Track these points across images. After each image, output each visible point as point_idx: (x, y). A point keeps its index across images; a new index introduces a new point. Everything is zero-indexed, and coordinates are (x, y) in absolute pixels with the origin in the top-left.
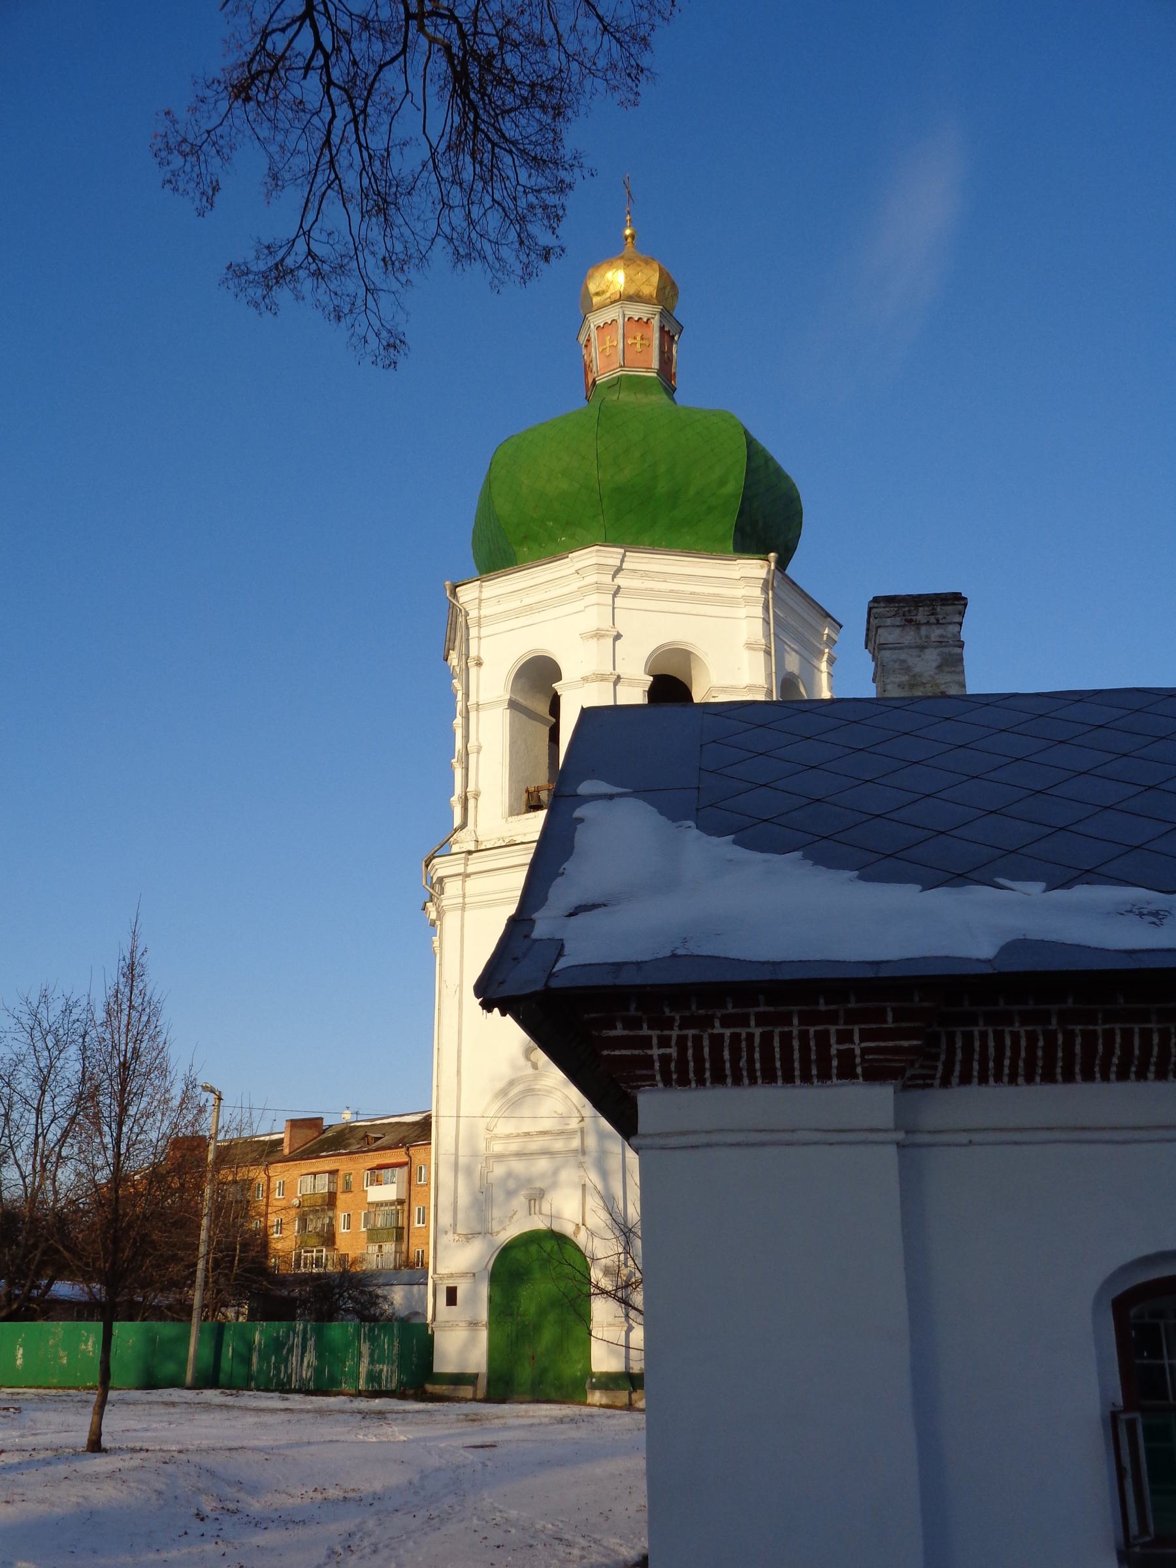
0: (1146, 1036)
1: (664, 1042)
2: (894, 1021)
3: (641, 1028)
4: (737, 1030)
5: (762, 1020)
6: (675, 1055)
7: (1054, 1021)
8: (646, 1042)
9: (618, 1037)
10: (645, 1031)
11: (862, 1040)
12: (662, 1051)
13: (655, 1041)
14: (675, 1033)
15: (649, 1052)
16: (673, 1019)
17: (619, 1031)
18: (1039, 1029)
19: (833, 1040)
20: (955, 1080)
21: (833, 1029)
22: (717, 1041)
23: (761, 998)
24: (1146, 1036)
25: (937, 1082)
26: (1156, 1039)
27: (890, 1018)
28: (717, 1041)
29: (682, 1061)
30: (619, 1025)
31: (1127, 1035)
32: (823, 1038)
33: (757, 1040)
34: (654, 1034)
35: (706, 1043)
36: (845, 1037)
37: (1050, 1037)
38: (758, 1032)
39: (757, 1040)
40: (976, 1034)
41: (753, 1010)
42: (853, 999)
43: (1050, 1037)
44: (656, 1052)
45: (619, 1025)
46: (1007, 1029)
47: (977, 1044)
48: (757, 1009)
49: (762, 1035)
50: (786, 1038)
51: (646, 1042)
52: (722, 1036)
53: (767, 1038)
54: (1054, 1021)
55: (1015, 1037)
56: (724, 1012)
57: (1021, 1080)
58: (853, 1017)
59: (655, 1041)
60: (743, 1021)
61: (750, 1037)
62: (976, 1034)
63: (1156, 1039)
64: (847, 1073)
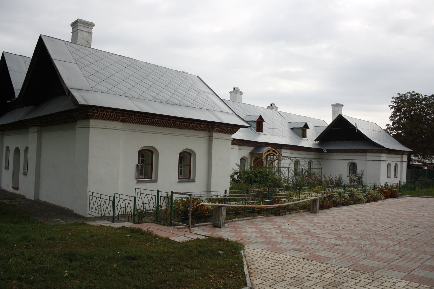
0: (150, 120)
1: (97, 113)
2: (126, 115)
3: (91, 110)
4: (107, 113)
5: (111, 112)
6: (98, 115)
7: (141, 117)
8: (95, 113)
9: (91, 112)
10: (95, 111)
11: (122, 116)
12: (97, 114)
13: (96, 113)
14: (99, 112)
15: (95, 114)
16: (99, 110)
17: (92, 111)
18: (139, 117)
19: (118, 116)
20: (127, 122)
21: (118, 115)
22: (104, 114)
23: (166, 117)
24: (150, 120)
25: (125, 122)
26: (151, 120)
27: (126, 114)
28: (104, 114)
29: (98, 116)
30: (92, 110)
31: (148, 119)
32: (117, 115)
33: (109, 115)
34: (96, 112)
35: (103, 114)
36: (120, 116)
37: (140, 119)
38: (134, 117)
39: (109, 115)
40: (114, 115)
41: (109, 111)
42: (158, 116)
43: (140, 119)
44: (96, 114)
45: (92, 110)
46: (136, 117)
47: (132, 118)
48: (110, 111)
49: (110, 114)
50: (113, 115)
51: (95, 113)
52: (105, 113)
53: (110, 114)
54: (141, 117)
55: (136, 118)
56: (142, 115)
57: (135, 123)
58: (121, 113)
59: (96, 113)
60: (108, 112)
61: (108, 114)
62: (114, 115)
63: (151, 120)
64: (118, 121)
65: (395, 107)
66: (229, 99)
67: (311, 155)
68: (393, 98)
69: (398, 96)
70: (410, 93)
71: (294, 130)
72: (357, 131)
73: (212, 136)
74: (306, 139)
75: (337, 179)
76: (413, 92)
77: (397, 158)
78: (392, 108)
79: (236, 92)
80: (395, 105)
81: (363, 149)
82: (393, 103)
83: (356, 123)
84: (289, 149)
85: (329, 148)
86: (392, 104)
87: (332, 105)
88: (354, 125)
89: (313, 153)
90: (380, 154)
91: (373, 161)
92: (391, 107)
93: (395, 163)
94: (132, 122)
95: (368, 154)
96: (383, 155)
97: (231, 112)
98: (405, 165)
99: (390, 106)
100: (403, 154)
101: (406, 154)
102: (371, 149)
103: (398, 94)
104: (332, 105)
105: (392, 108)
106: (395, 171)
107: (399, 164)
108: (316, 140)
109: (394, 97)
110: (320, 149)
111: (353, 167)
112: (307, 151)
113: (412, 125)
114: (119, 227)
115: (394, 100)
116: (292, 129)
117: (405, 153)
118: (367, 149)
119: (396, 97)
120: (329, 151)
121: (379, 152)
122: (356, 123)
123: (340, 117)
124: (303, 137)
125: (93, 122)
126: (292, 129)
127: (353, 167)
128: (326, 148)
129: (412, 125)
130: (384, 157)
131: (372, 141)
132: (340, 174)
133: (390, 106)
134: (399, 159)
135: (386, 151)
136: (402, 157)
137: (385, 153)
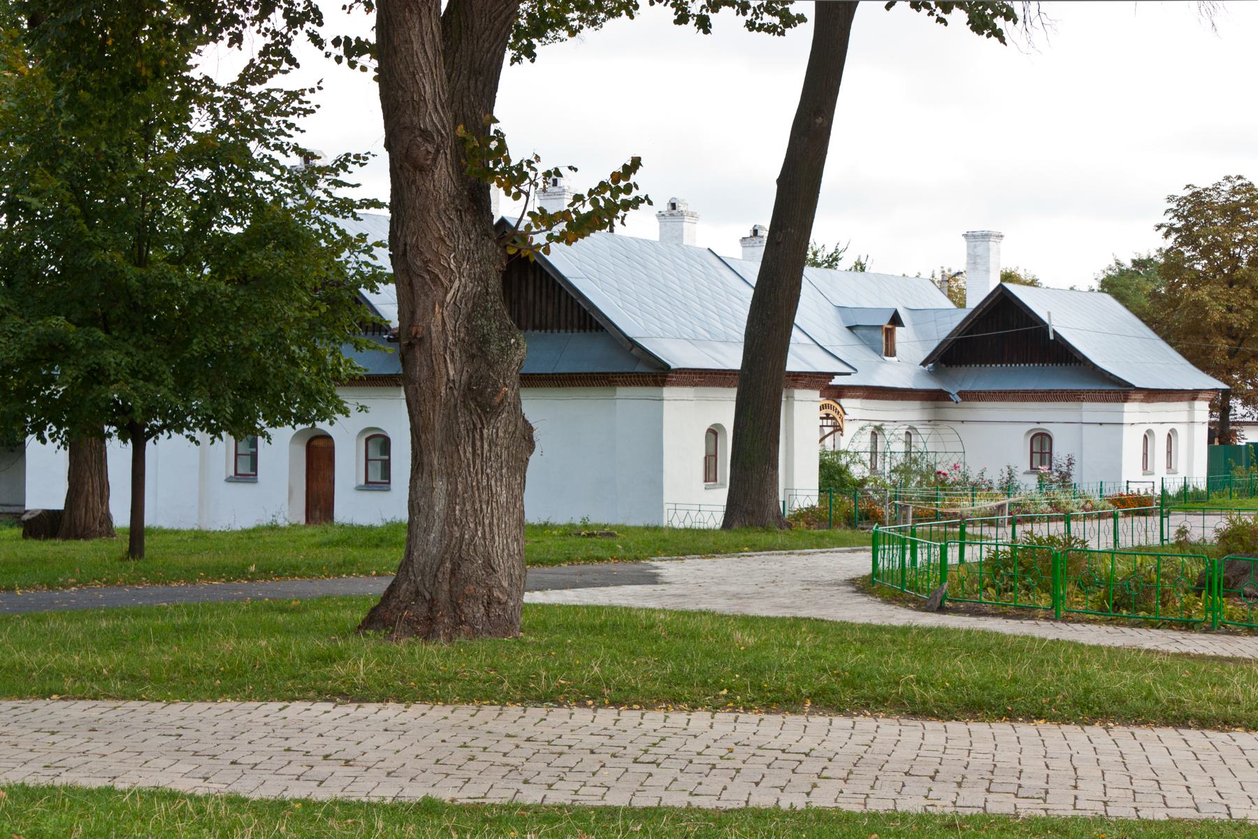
65: (1177, 230)
66: (657, 238)
67: (911, 412)
68: (1170, 199)
69: (1188, 193)
70: (1227, 178)
71: (858, 332)
72: (1052, 337)
73: (793, 397)
74: (895, 359)
75: (1005, 480)
76: (1240, 177)
77: (1175, 412)
78: (1167, 235)
79: (682, 214)
80: (1179, 224)
81: (1072, 391)
82: (1172, 215)
83: (1049, 313)
84: (857, 397)
85: (968, 386)
86: (1166, 220)
87: (966, 236)
88: (1045, 318)
89: (916, 404)
90: (1121, 404)
91: (1101, 424)
92: (1164, 230)
93: (1167, 428)
94: (841, 412)
95: (1086, 405)
96: (1128, 406)
97: (811, 342)
98: (1202, 434)
99: (1159, 227)
100: (1194, 399)
101: (1205, 400)
102: (1095, 391)
103: (1188, 186)
104: (966, 236)
105: (1167, 235)
106: (1169, 452)
107: (1182, 430)
108: (924, 363)
109: (1174, 196)
110: (941, 391)
111: (1041, 443)
112: (903, 399)
113: (1228, 300)
114: (687, 561)
115: (1174, 206)
116: (851, 328)
117: (1200, 396)
118: (1082, 392)
119: (1180, 196)
120: (966, 396)
121: (1117, 400)
122: (1049, 313)
123: (1001, 294)
124: (887, 355)
125: (668, 392)
126: (851, 328)
127: (1041, 443)
128: (958, 389)
129: (1228, 300)
130: (1132, 411)
131: (1095, 367)
132: (1012, 468)
133: (1159, 227)
134: (1184, 417)
135: (1140, 396)
136: (1192, 409)
137: (1135, 400)
